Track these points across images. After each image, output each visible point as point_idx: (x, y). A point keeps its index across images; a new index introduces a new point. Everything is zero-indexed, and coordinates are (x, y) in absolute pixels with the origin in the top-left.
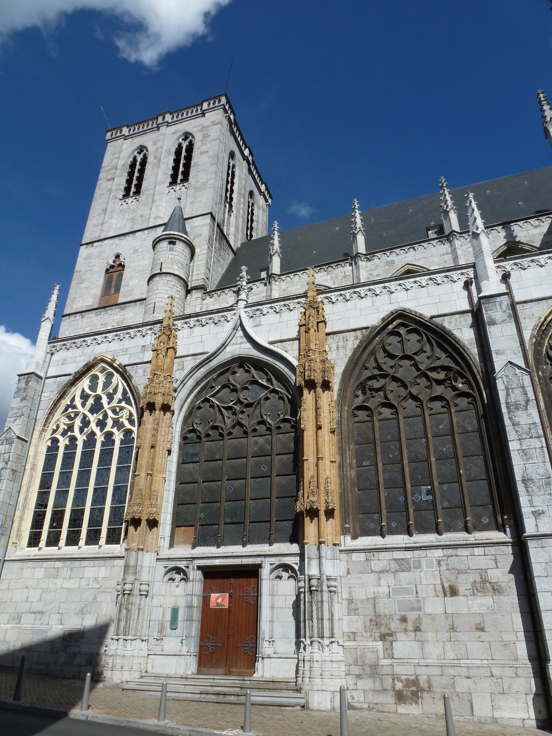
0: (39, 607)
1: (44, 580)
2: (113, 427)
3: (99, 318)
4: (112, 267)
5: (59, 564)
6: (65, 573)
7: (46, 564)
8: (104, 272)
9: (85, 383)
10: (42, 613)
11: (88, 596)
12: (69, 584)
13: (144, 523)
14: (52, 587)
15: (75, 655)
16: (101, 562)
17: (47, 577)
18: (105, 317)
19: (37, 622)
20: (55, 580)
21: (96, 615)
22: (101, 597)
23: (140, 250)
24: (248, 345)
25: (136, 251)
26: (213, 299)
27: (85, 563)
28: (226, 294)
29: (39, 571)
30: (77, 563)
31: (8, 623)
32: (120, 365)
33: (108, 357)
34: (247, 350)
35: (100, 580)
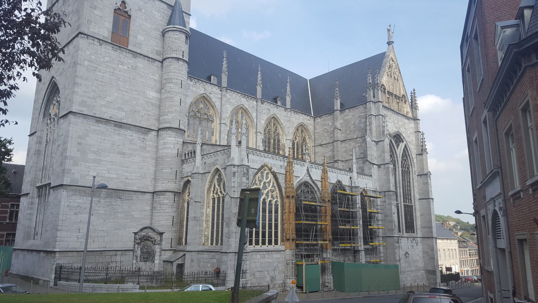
0: (260, 269)
1: (261, 259)
2: (271, 198)
3: (116, 54)
4: (119, 9)
5: (265, 253)
6: (267, 256)
7: (260, 253)
8: (113, 11)
9: (259, 174)
10: (262, 271)
11: (275, 264)
12: (270, 260)
13: (291, 240)
14: (263, 261)
15: (275, 284)
16: (278, 252)
17: (261, 258)
18: (121, 55)
19: (261, 275)
20: (264, 259)
21: (278, 271)
22: (279, 265)
23: (143, 11)
24: (309, 178)
25: (140, 9)
26: (192, 83)
27: (273, 253)
28: (200, 84)
29: (258, 256)
30: (270, 253)
31: (251, 276)
32: (274, 171)
33: (269, 166)
34: (308, 179)
35: (278, 259)
